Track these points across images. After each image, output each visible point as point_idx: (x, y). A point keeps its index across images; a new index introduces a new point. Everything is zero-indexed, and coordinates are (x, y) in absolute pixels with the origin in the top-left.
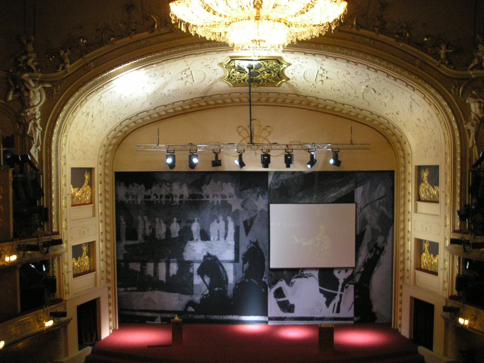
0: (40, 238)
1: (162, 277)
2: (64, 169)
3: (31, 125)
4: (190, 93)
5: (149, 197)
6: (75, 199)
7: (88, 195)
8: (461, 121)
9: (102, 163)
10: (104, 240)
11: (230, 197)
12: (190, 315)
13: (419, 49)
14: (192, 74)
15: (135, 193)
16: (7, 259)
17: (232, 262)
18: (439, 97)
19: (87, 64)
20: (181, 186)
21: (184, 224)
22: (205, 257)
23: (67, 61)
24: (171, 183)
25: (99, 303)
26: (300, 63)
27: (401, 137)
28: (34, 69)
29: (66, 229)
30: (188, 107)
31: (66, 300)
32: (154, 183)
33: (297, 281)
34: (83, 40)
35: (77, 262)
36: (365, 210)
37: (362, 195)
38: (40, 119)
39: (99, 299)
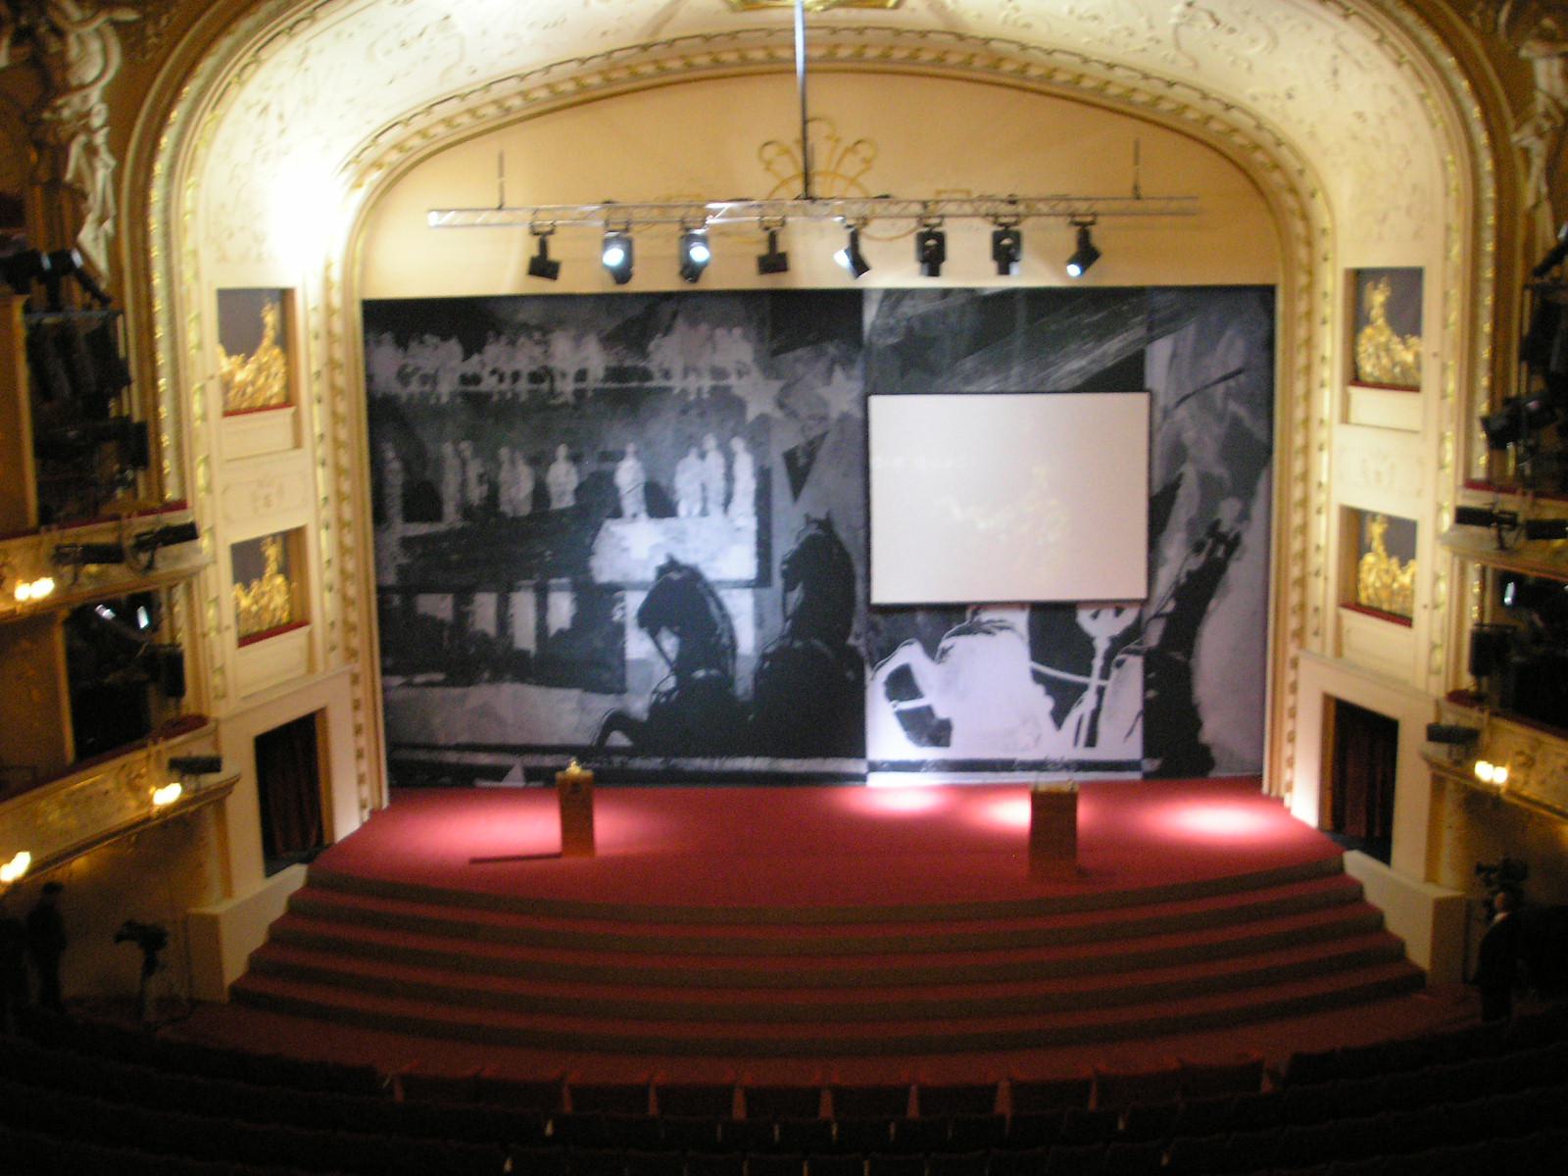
0: (125, 521)
1: (525, 637)
3: (75, 150)
5: (476, 380)
6: (236, 390)
8: (1503, 124)
12: (617, 760)
15: (429, 369)
17: (747, 585)
18: (1430, 38)
20: (578, 340)
21: (591, 465)
22: (662, 571)
25: (325, 721)
27: (1301, 172)
29: (209, 489)
30: (595, 80)
31: (217, 721)
32: (491, 333)
33: (960, 646)
36: (1182, 413)
39: (322, 711)
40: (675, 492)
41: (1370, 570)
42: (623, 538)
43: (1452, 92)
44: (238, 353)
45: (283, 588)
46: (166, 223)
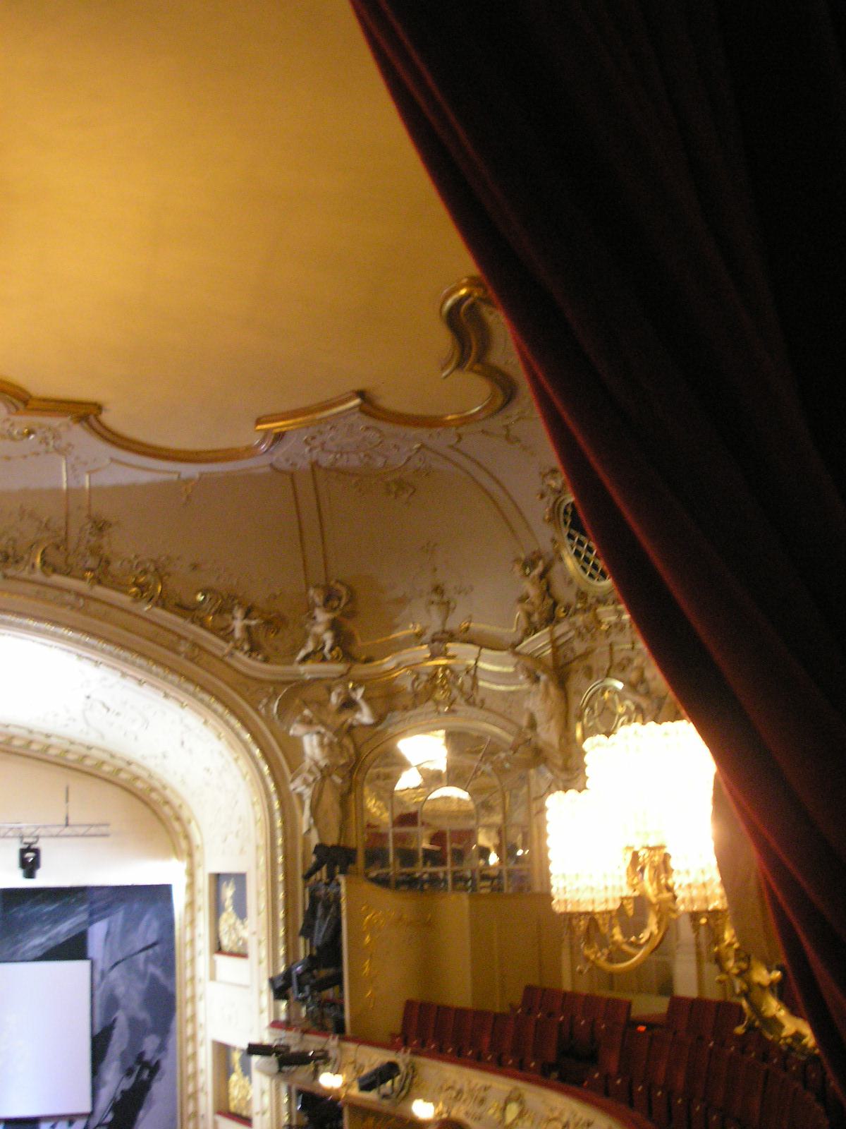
8: (283, 774)
13: (185, 618)
36: (114, 974)
37: (106, 940)
41: (235, 1086)
43: (253, 756)
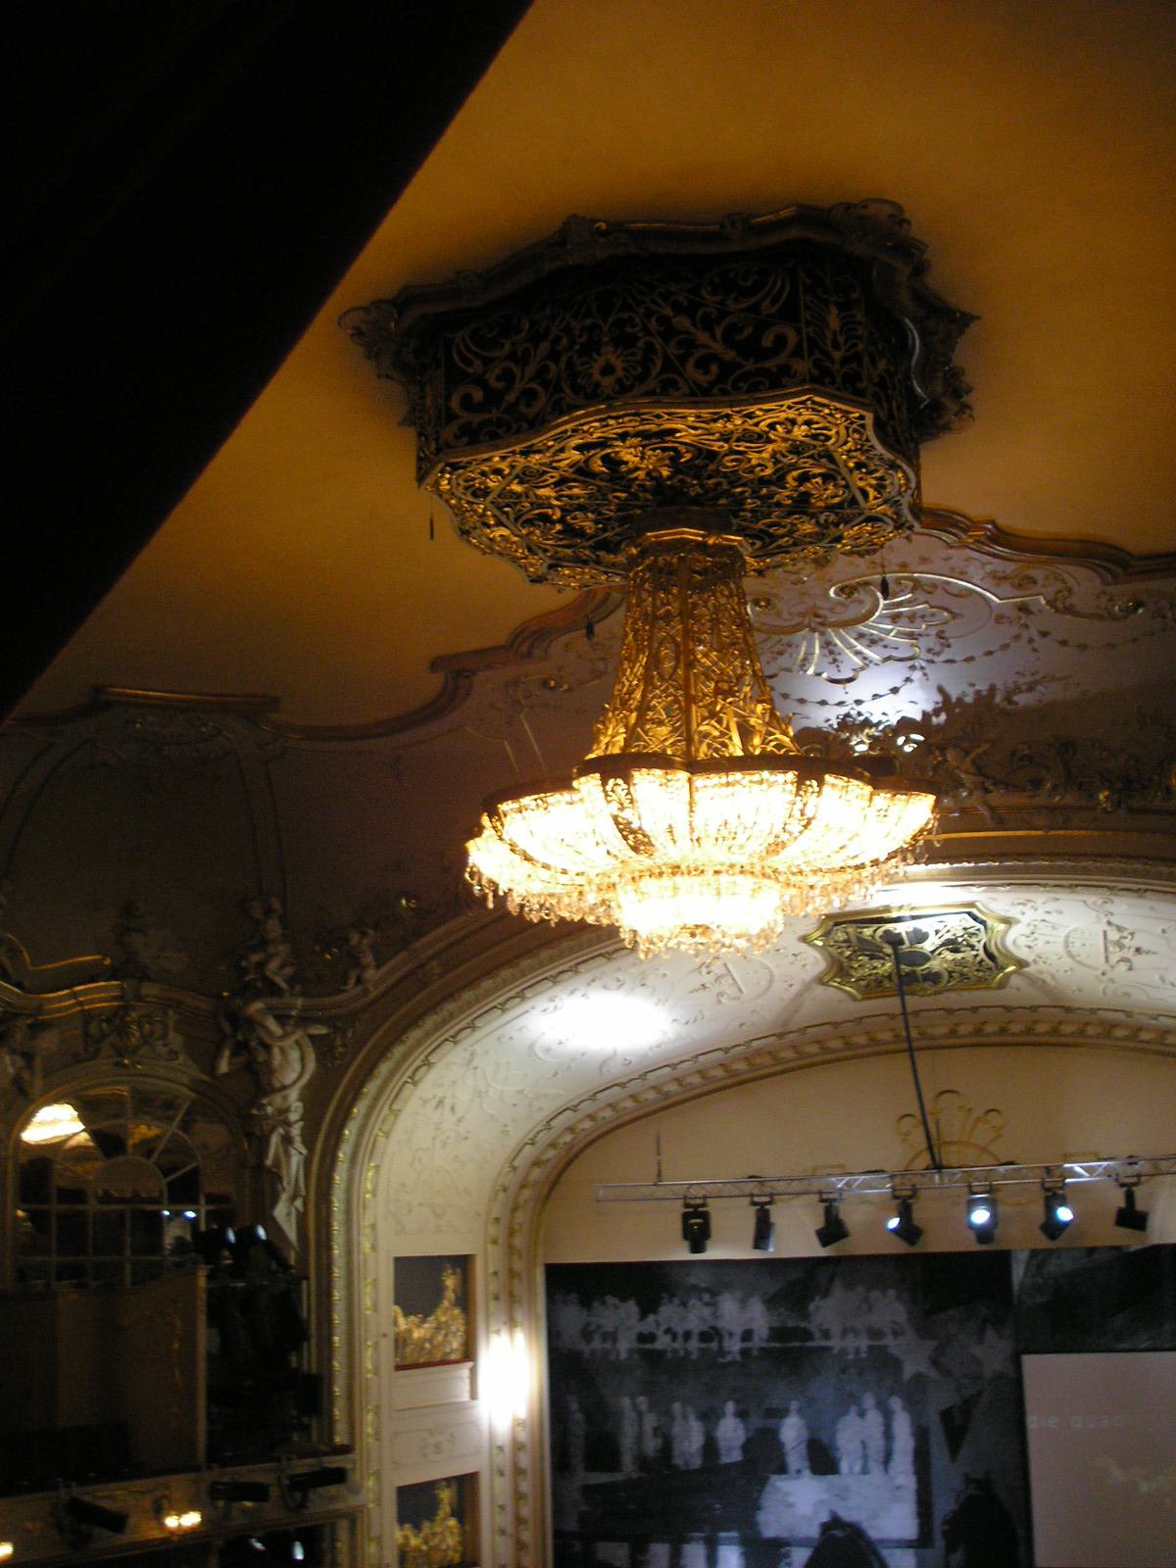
0: (285, 1463)
2: (371, 1264)
3: (275, 1139)
4: (742, 1025)
5: (651, 1338)
7: (454, 1333)
9: (500, 1241)
10: (508, 1470)
11: (896, 1334)
14: (729, 972)
16: (171, 1522)
19: (422, 966)
20: (743, 1302)
22: (826, 1528)
23: (368, 959)
24: (714, 1293)
26: (1040, 915)
28: (284, 985)
29: (378, 1436)
30: (742, 1066)
34: (408, 901)
35: (416, 1535)
38: (301, 1123)
40: (837, 1449)
42: (788, 1494)
44: (415, 1314)
45: (456, 1531)
46: (348, 1201)
